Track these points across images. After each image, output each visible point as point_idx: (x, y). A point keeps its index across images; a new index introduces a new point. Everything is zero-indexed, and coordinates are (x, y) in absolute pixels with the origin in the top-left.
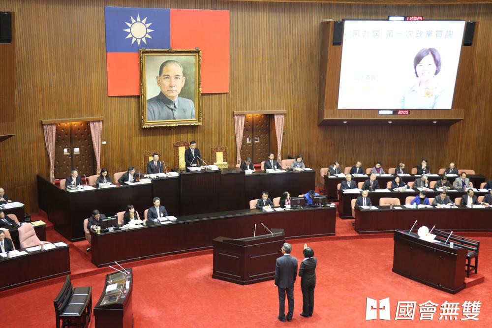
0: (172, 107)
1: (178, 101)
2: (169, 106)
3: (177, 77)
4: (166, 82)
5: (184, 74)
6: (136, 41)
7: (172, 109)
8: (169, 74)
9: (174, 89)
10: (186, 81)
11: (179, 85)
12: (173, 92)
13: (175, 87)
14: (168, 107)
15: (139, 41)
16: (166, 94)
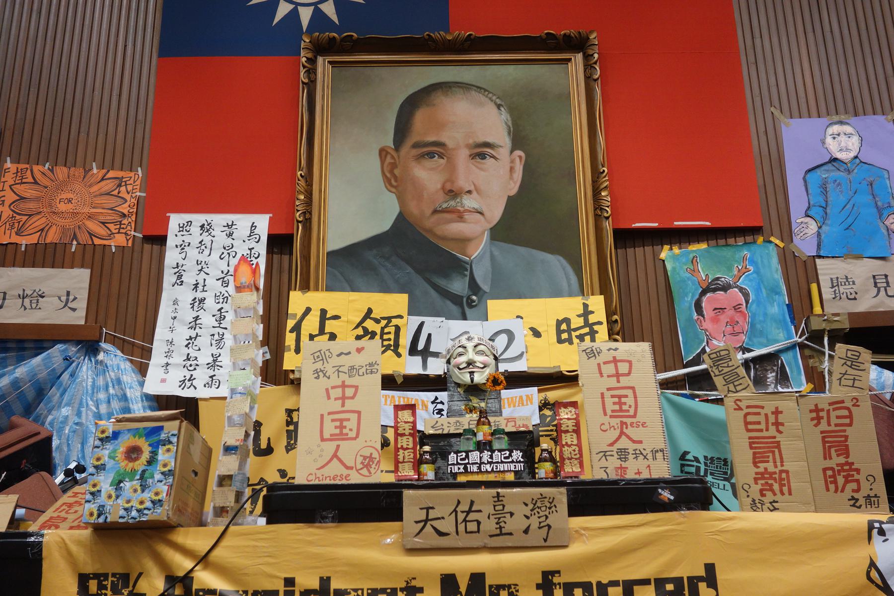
0: (458, 286)
1: (492, 258)
2: (442, 282)
3: (481, 151)
4: (428, 176)
5: (518, 141)
6: (294, 15)
7: (456, 300)
8: (444, 138)
9: (469, 202)
10: (527, 169)
11: (492, 186)
12: (460, 215)
13: (475, 193)
14: (436, 287)
15: (305, 15)
16: (430, 222)
